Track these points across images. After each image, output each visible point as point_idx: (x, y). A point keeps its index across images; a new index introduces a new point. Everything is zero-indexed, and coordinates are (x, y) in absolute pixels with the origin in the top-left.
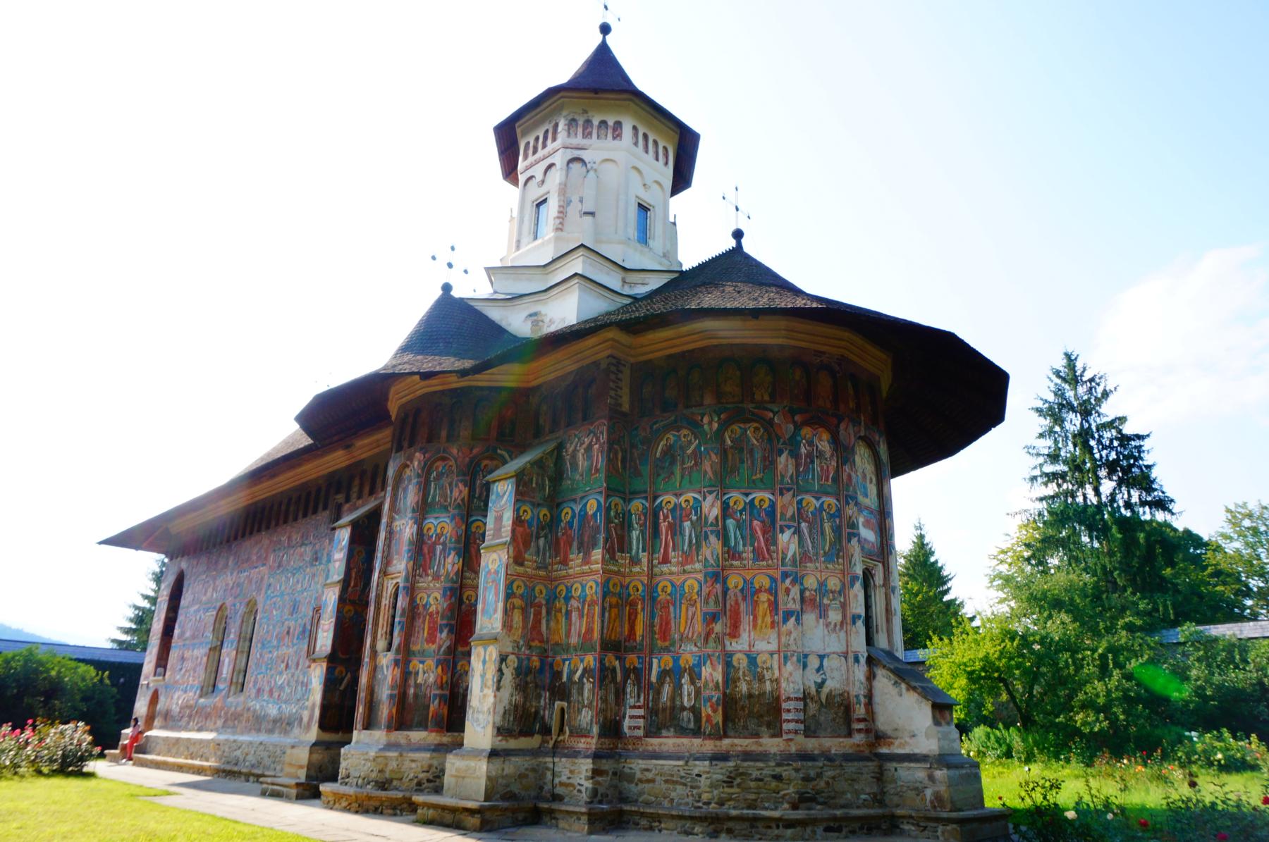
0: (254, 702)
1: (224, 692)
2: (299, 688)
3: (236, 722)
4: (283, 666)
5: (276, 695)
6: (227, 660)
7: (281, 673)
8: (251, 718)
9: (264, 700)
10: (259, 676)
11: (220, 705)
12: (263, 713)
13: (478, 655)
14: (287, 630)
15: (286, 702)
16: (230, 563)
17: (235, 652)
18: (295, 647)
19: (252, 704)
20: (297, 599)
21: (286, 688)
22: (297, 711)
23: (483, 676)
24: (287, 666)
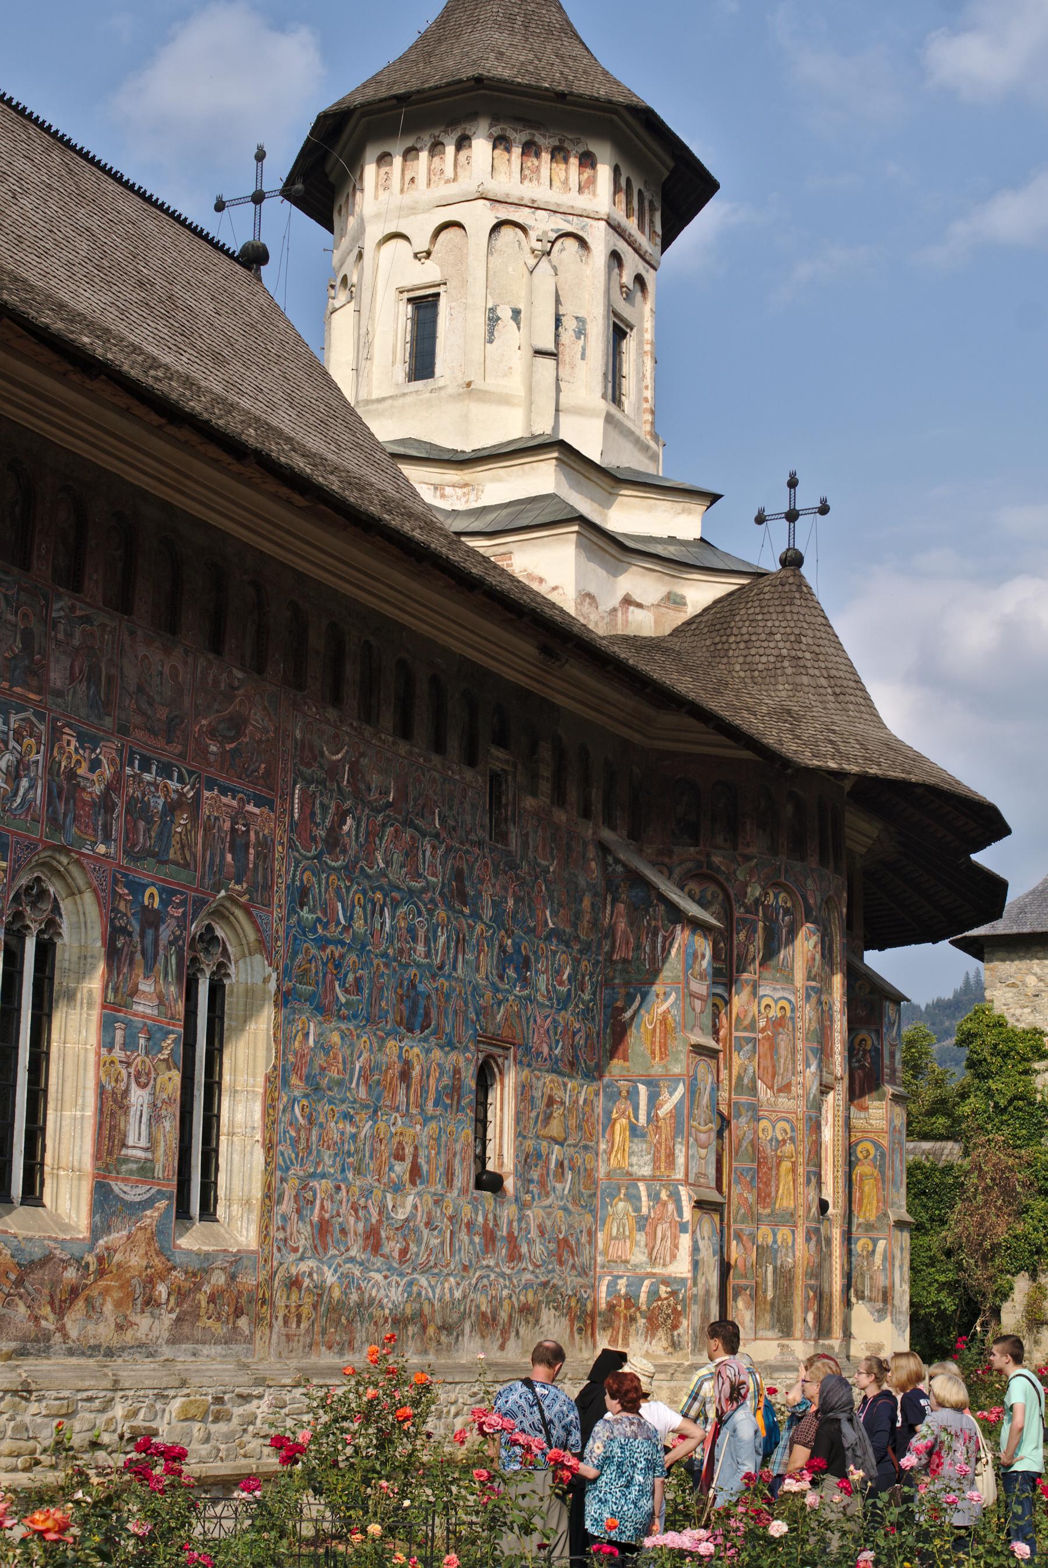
0: (312, 1263)
1: (151, 1217)
2: (464, 1236)
3: (243, 1322)
4: (401, 1169)
5: (392, 1247)
6: (138, 1097)
7: (397, 1188)
8: (305, 1310)
9: (352, 1260)
10: (314, 1183)
11: (136, 1260)
12: (354, 1297)
13: (897, 1240)
14: (398, 1067)
15: (425, 1270)
16: (57, 677)
17: (176, 1076)
18: (433, 1125)
19: (304, 1267)
20: (421, 988)
21: (426, 1232)
22: (465, 1297)
23: (901, 1267)
24: (415, 1172)
